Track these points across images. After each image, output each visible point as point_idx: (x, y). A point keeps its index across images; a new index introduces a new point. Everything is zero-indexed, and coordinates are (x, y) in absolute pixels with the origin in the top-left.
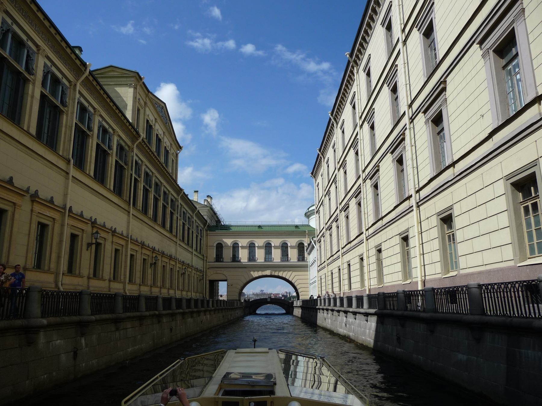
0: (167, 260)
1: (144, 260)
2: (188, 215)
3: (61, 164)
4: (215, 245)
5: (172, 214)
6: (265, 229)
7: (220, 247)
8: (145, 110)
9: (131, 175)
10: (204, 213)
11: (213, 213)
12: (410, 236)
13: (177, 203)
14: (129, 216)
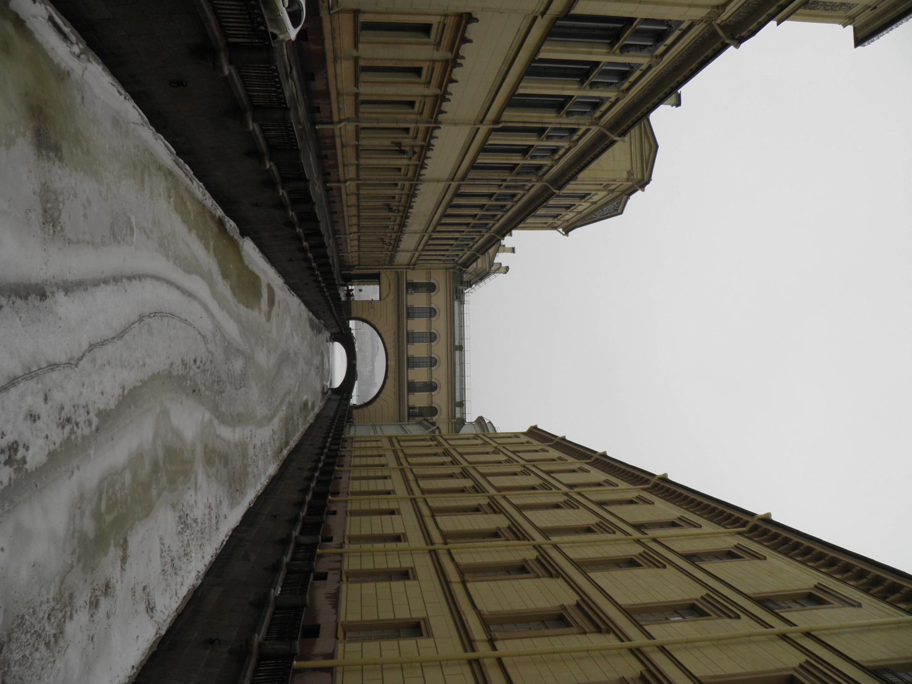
0: (398, 222)
1: (394, 197)
2: (471, 244)
3: (491, 115)
4: (432, 281)
5: (468, 224)
7: (431, 288)
8: (602, 190)
9: (505, 180)
10: (480, 264)
11: (482, 276)
12: (399, 544)
13: (484, 230)
14: (447, 180)
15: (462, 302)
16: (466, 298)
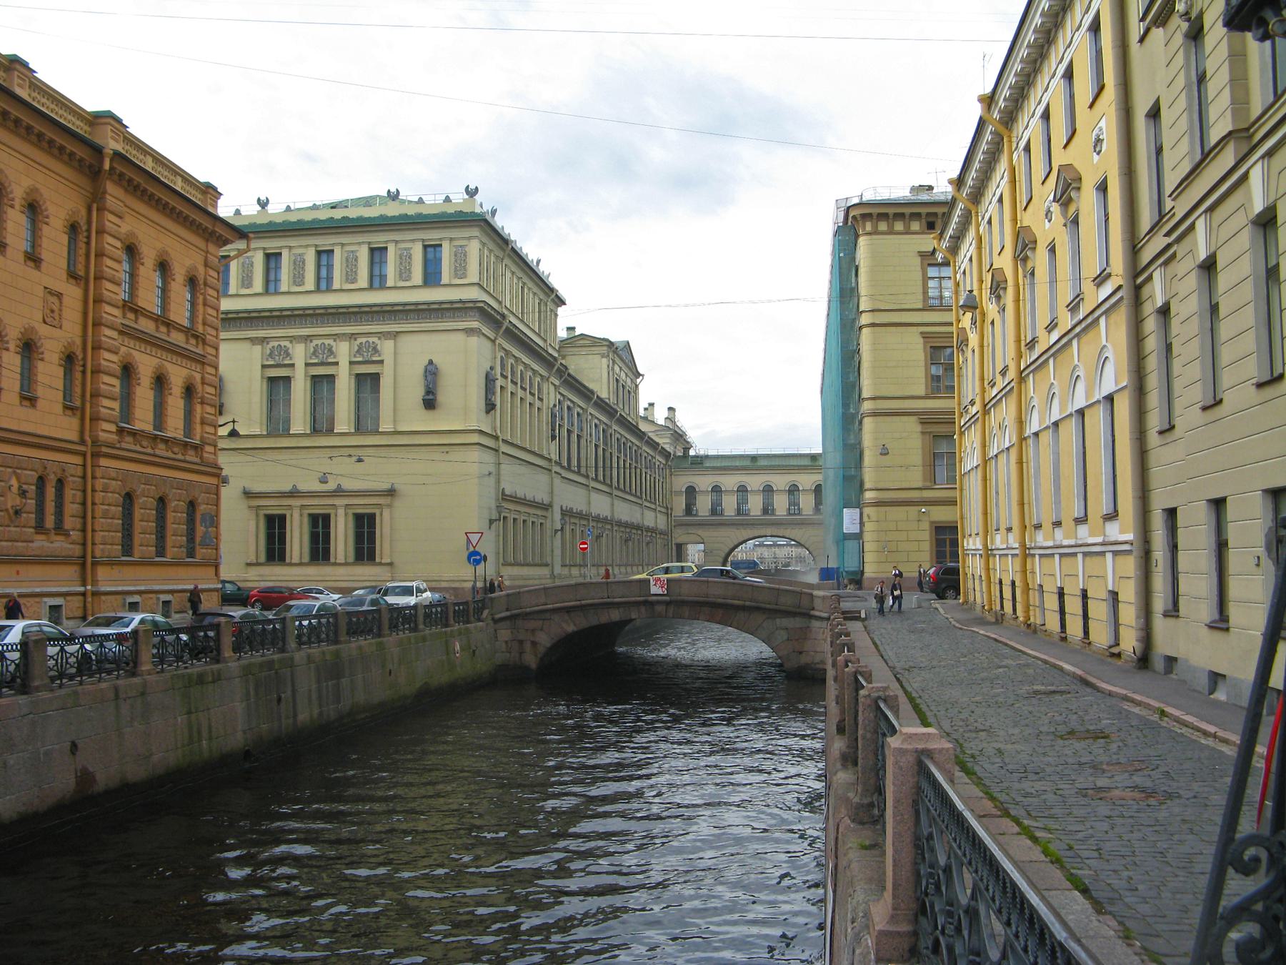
6: (762, 463)
7: (691, 492)
10: (665, 442)
11: (679, 437)
15: (707, 457)
16: (702, 453)
